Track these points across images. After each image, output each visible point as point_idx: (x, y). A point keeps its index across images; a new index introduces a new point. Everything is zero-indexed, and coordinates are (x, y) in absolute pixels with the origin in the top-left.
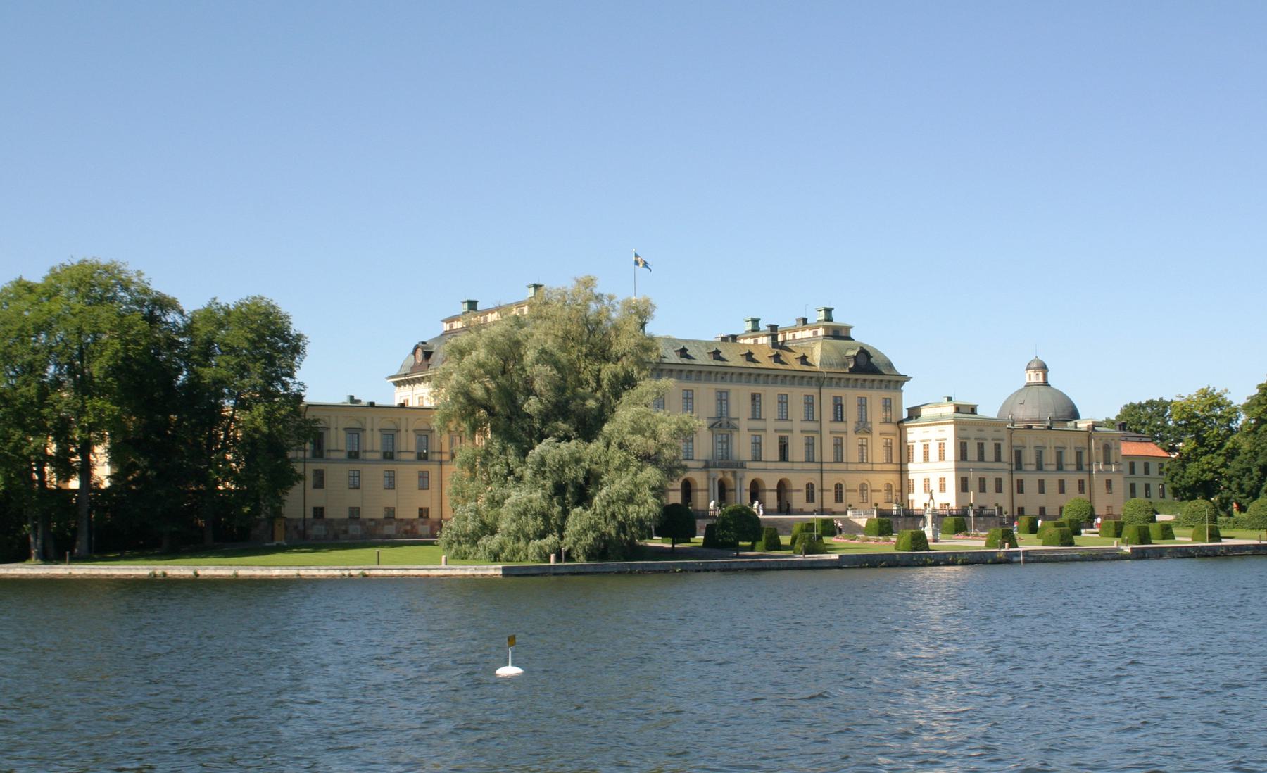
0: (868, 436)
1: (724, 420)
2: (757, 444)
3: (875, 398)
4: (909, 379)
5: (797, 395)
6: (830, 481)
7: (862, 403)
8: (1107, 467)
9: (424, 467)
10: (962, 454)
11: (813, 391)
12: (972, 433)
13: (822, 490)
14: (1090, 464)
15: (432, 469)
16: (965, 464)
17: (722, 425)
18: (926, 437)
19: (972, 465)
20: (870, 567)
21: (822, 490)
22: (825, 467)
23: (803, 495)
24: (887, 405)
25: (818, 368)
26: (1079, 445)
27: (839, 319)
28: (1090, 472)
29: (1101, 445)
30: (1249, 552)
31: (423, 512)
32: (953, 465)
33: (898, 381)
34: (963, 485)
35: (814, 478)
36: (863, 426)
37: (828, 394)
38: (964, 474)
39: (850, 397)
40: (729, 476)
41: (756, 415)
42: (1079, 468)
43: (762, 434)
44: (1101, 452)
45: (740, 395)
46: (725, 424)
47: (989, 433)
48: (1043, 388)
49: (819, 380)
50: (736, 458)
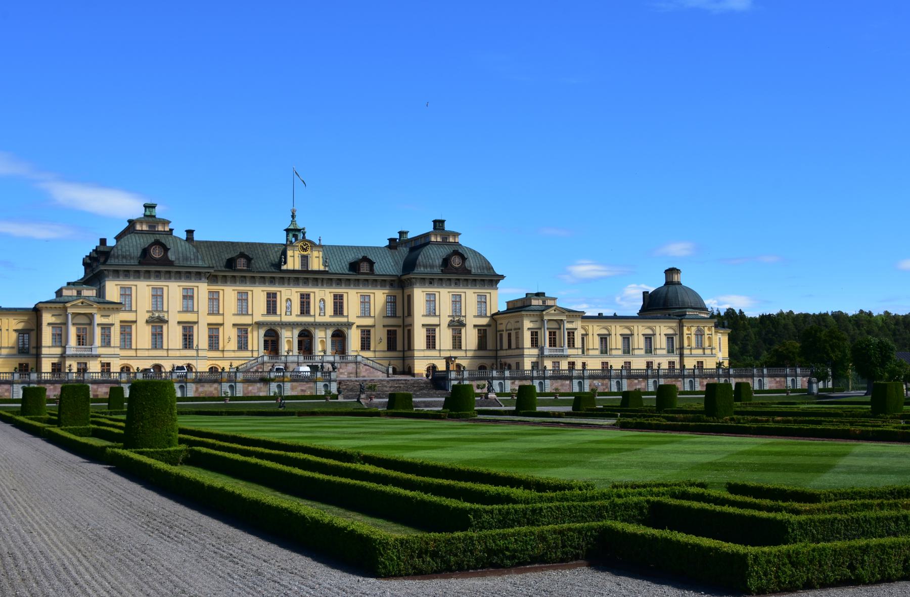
3: (470, 296)
4: (502, 277)
7: (457, 301)
14: (682, 348)
18: (509, 327)
22: (416, 354)
24: (482, 301)
26: (671, 332)
37: (419, 295)
42: (671, 351)
44: (693, 338)
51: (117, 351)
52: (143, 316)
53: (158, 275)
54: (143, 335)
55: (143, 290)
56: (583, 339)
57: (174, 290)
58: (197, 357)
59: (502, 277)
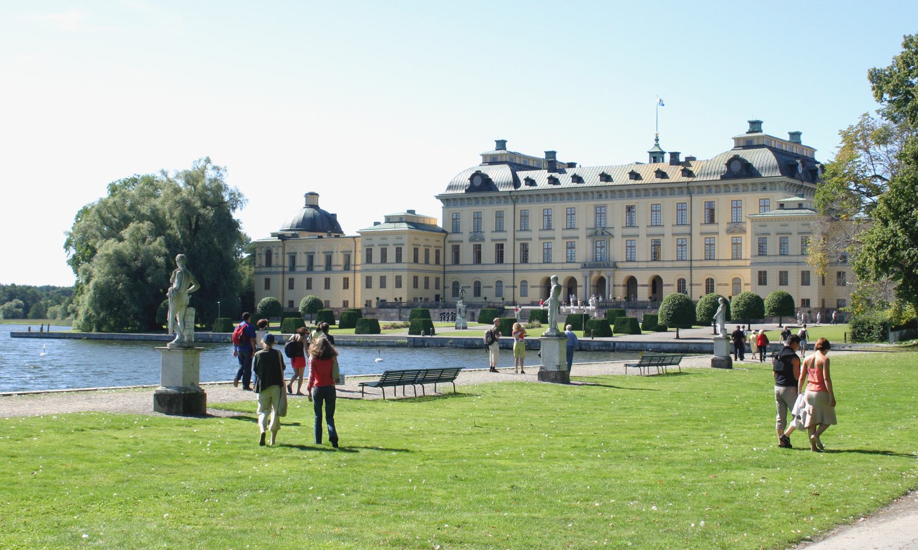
1: (599, 230)
2: (630, 248)
5: (669, 204)
6: (700, 277)
7: (736, 207)
9: (346, 275)
11: (685, 199)
15: (350, 275)
17: (600, 234)
22: (694, 264)
31: (346, 303)
35: (685, 274)
37: (699, 202)
39: (723, 203)
40: (603, 274)
41: (631, 224)
43: (716, 236)
46: (599, 233)
51: (406, 266)
54: (467, 254)
55: (466, 214)
57: (488, 212)
58: (505, 271)
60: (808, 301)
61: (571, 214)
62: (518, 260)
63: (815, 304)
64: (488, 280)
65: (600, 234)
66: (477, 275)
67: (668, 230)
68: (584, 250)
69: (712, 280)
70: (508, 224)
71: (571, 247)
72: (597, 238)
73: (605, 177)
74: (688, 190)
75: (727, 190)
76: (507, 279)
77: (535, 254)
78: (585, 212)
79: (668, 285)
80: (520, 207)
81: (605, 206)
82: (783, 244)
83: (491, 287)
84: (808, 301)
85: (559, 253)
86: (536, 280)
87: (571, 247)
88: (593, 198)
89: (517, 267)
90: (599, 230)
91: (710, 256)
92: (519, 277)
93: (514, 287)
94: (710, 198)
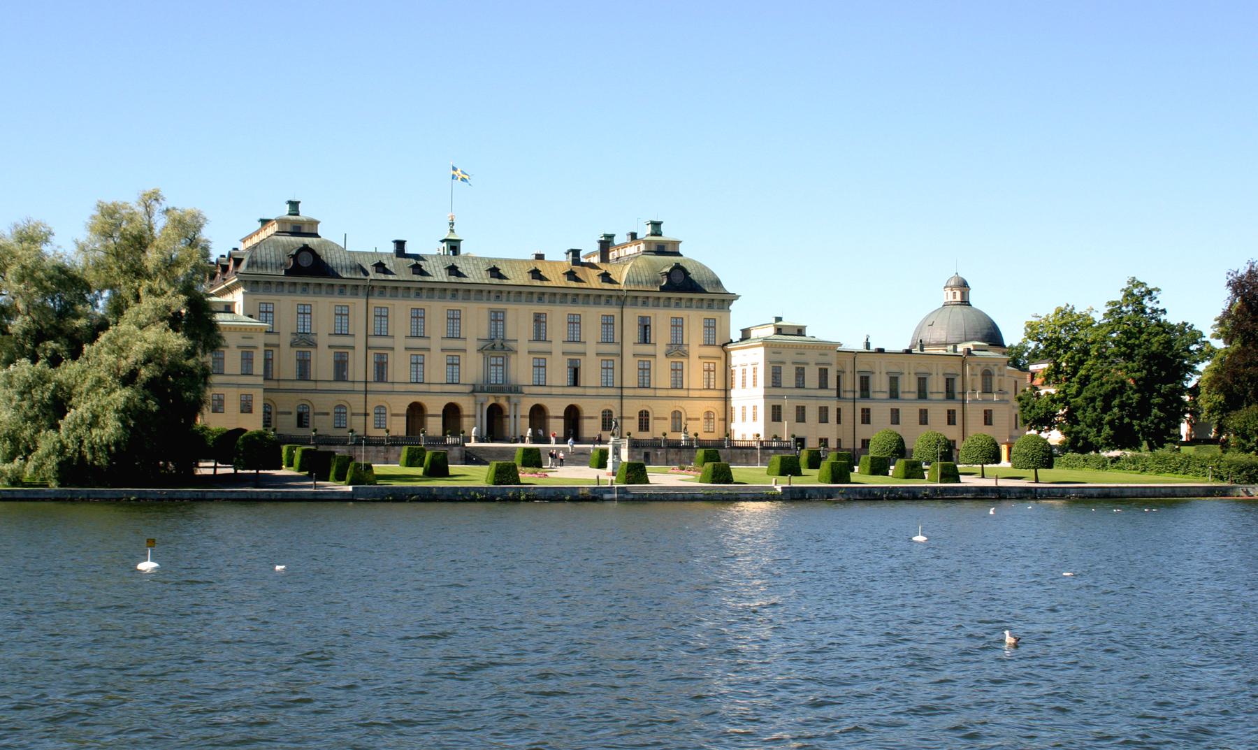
0: (685, 361)
1: (498, 342)
2: (540, 366)
3: (694, 320)
4: (737, 297)
5: (592, 316)
6: (632, 408)
7: (677, 325)
8: (987, 396)
10: (775, 379)
11: (613, 311)
12: (789, 356)
13: (622, 418)
14: (964, 393)
16: (777, 391)
17: (497, 347)
19: (789, 392)
20: (393, 501)
21: (622, 418)
22: (626, 392)
23: (598, 423)
24: (710, 326)
25: (622, 286)
26: (950, 371)
27: (668, 234)
28: (964, 401)
29: (979, 371)
30: (969, 496)
32: (760, 390)
33: (725, 300)
34: (775, 414)
35: (613, 405)
36: (677, 349)
37: (632, 316)
38: (776, 402)
39: (661, 319)
40: (503, 402)
42: (950, 395)
44: (979, 380)
45: (519, 319)
46: (498, 346)
47: (811, 357)
48: (965, 309)
49: (621, 300)
50: (513, 383)
52: (286, 339)
53: (305, 288)
55: (287, 305)
56: (838, 377)
57: (324, 306)
59: (734, 297)
60: (826, 440)
61: (454, 318)
62: (371, 377)
63: (832, 444)
64: (323, 403)
65: (497, 347)
66: (304, 396)
67: (591, 347)
68: (473, 368)
69: (647, 413)
70: (357, 324)
71: (453, 364)
72: (495, 353)
73: (495, 272)
74: (621, 300)
75: (667, 304)
76: (356, 403)
77: (399, 368)
78: (476, 318)
79: (591, 418)
80: (375, 302)
81: (503, 312)
82: (800, 373)
83: (327, 414)
84: (826, 440)
85: (436, 369)
86: (401, 405)
87: (453, 364)
88: (488, 299)
89: (371, 387)
90: (498, 342)
91: (678, 385)
92: (373, 400)
93: (366, 414)
94: (645, 312)
